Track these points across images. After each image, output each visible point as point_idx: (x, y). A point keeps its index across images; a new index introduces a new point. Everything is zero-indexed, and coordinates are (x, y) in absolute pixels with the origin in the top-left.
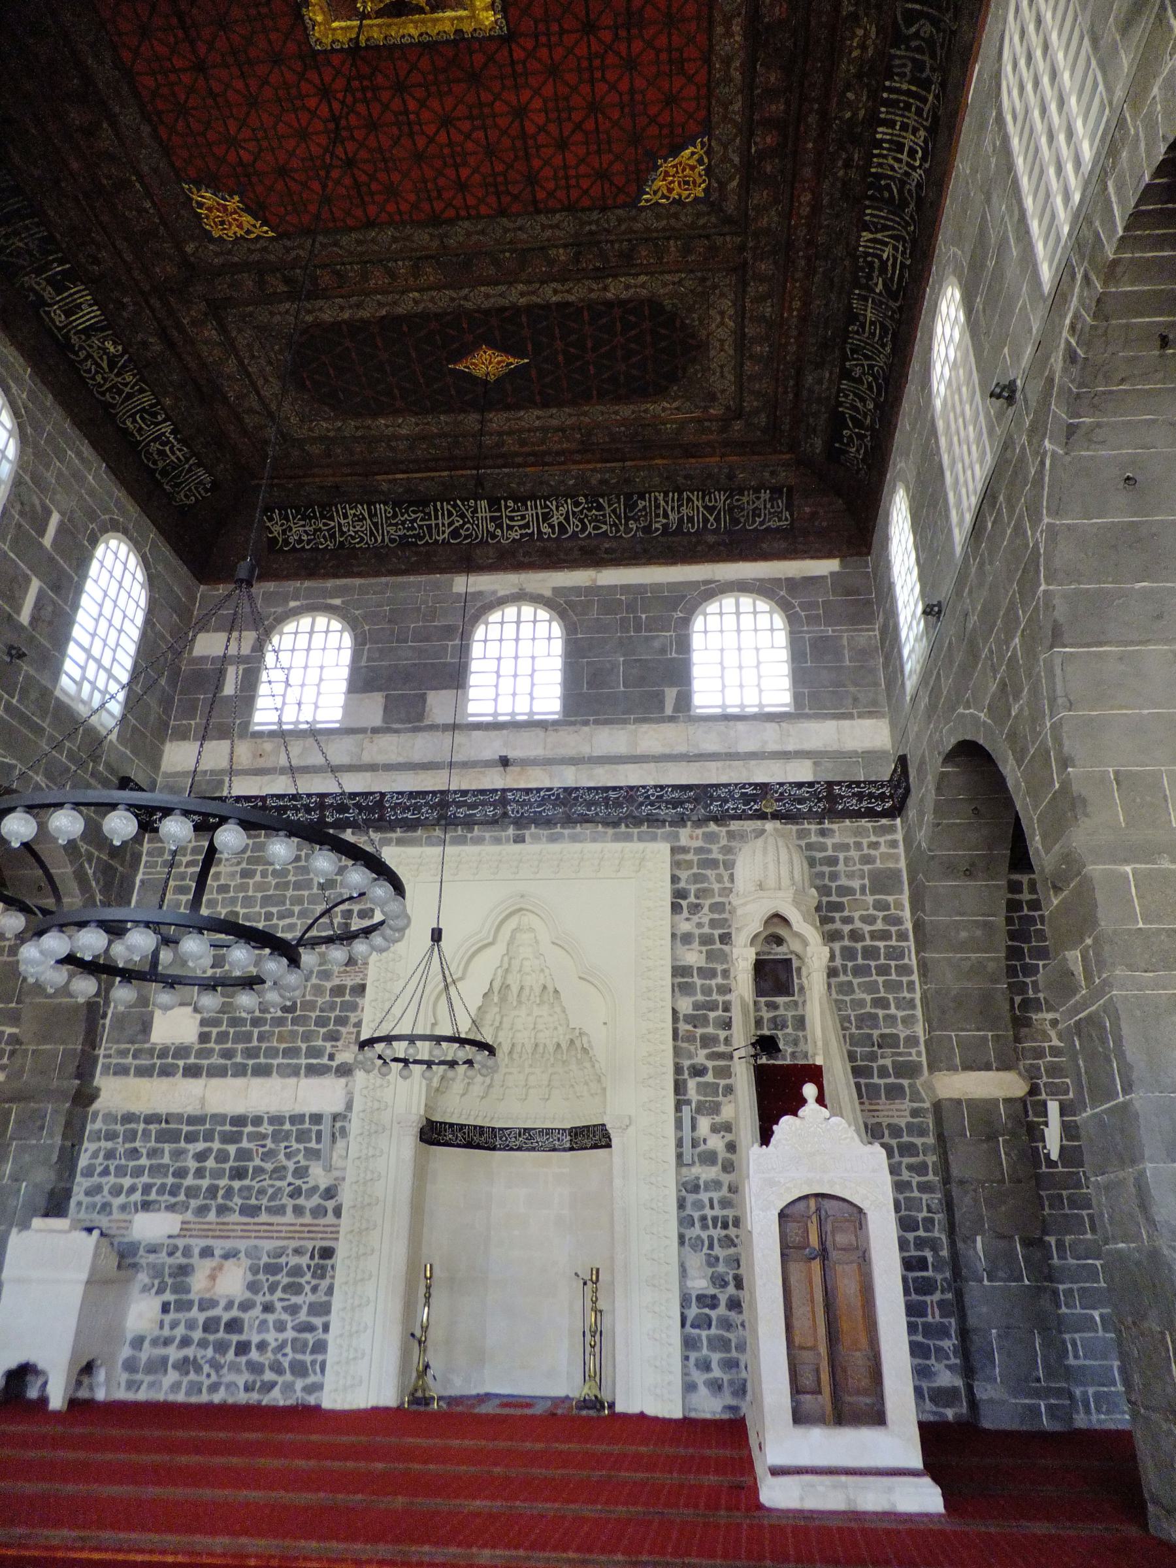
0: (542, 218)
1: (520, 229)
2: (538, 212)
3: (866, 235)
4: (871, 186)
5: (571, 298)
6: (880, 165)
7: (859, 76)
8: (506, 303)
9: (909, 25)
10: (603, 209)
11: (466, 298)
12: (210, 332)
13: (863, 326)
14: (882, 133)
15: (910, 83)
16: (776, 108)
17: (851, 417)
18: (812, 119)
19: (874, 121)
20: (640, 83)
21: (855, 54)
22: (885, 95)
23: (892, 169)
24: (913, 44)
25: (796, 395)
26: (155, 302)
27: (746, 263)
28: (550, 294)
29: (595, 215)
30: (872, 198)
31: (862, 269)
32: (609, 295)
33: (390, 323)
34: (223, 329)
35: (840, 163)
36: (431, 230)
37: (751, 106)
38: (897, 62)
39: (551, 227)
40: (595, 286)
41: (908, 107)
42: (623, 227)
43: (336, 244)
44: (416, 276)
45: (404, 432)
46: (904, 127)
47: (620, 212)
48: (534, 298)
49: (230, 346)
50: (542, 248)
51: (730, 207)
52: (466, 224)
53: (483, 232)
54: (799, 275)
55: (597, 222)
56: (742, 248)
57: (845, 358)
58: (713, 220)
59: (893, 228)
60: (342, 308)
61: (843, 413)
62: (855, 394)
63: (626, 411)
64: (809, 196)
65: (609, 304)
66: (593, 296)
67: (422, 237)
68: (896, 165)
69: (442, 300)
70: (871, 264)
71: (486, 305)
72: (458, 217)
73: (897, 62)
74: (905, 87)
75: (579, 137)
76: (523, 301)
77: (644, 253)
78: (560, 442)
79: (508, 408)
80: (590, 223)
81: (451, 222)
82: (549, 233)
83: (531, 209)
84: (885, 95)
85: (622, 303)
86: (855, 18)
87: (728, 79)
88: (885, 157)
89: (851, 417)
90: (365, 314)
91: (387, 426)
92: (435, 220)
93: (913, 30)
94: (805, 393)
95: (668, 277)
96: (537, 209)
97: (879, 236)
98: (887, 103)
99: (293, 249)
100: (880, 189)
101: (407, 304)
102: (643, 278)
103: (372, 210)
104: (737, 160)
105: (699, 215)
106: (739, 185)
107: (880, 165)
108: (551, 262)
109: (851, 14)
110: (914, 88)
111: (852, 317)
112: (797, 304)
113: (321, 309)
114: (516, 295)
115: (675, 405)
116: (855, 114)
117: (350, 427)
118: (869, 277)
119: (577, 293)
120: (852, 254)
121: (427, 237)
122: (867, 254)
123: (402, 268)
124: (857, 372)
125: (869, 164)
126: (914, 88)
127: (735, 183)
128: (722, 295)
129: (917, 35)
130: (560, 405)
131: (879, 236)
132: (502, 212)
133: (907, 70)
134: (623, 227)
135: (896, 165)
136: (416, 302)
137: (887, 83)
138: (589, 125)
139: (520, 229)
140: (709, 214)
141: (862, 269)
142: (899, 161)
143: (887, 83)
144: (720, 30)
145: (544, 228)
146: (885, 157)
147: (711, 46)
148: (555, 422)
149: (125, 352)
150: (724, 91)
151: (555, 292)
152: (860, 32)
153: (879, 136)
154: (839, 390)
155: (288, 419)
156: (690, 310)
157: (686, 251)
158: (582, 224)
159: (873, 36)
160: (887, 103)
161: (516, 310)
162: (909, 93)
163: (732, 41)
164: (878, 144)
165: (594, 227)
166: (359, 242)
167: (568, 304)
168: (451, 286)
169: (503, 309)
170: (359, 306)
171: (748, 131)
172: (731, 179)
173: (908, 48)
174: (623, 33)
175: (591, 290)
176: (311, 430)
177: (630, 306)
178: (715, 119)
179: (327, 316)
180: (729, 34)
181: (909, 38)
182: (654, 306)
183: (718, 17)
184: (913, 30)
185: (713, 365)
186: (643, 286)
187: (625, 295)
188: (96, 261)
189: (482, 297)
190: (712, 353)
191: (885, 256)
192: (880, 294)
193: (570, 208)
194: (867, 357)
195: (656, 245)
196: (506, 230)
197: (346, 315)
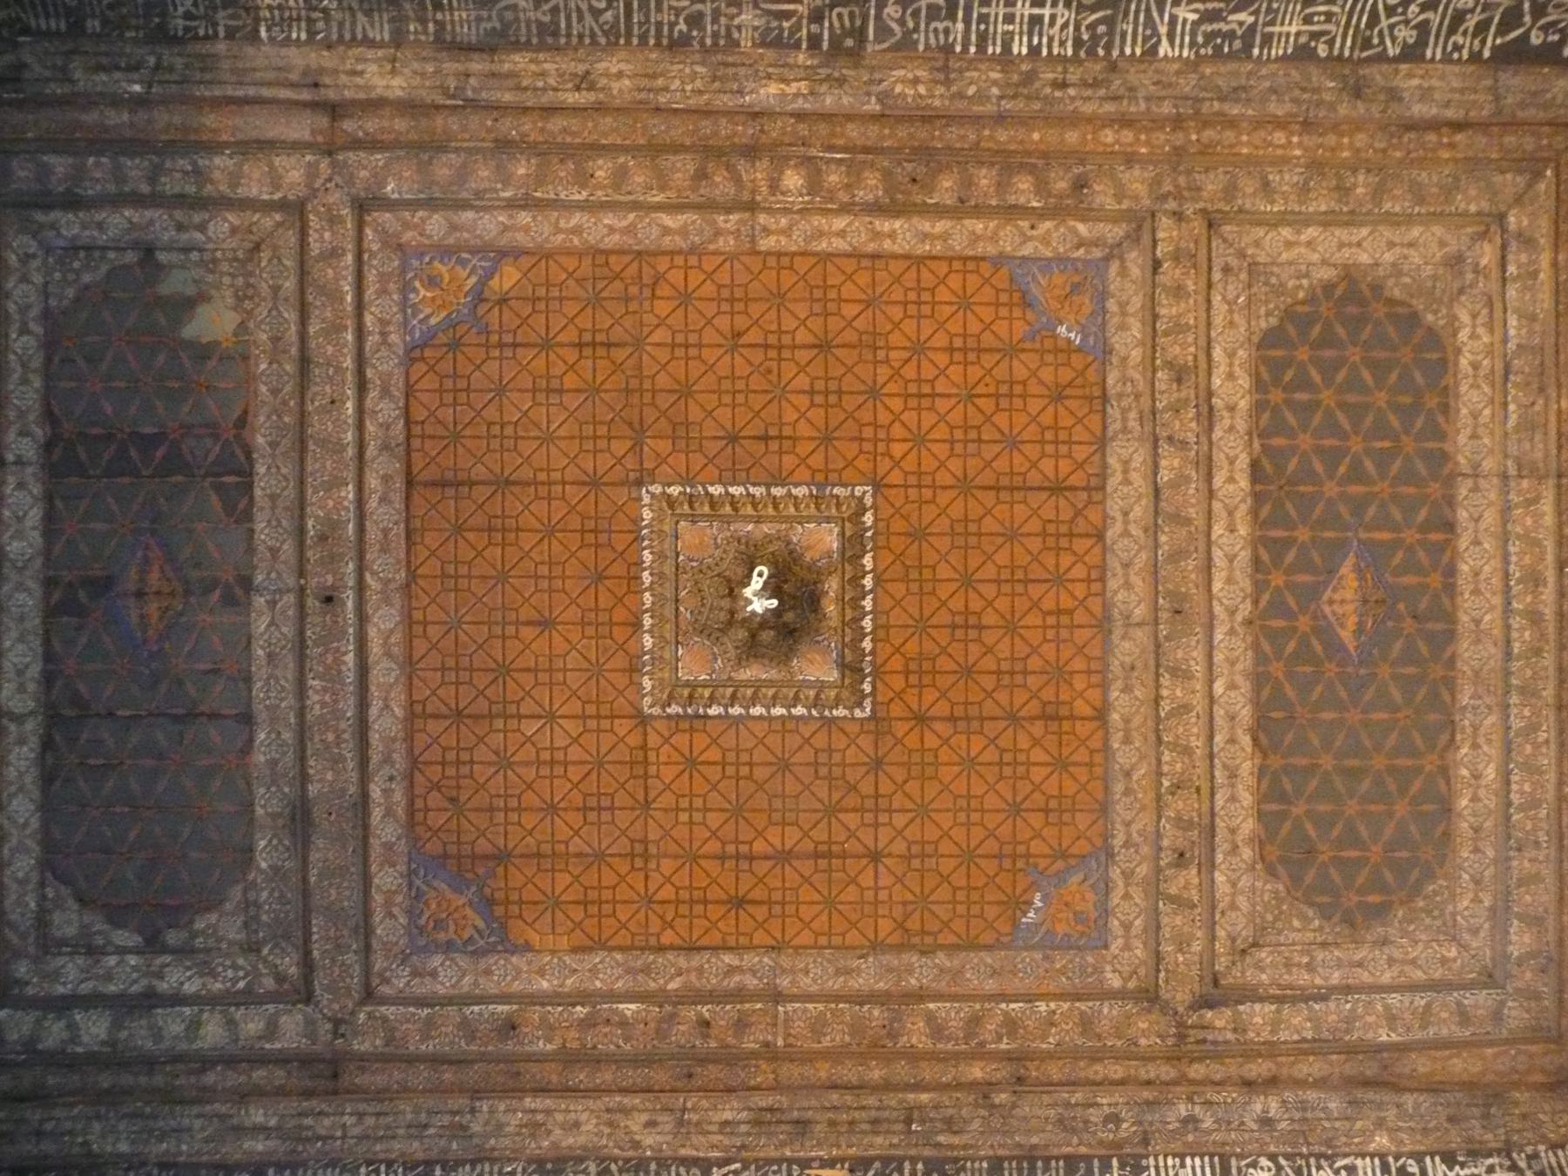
0: (1113, 482)
1: (1126, 514)
2: (1102, 488)
3: (1164, 49)
4: (1092, 53)
5: (1243, 461)
6: (1062, 44)
7: (947, 82)
8: (1244, 556)
9: (891, 32)
10: (1104, 398)
11: (1232, 612)
12: (1258, 1014)
13: (1315, 36)
14: (1020, 48)
15: (954, 21)
16: (985, 179)
17: (1501, 31)
18: (1002, 135)
19: (1006, 59)
20: (940, 340)
21: (922, 89)
22: (973, 49)
23: (1065, 26)
24: (911, 25)
25: (1458, 126)
26: (1197, 1071)
27: (1204, 211)
28: (1234, 485)
29: (1114, 412)
30: (1108, 47)
31: (1218, 49)
32: (1243, 404)
33: (1265, 732)
34: (1251, 994)
35: (1058, 94)
36: (1116, 637)
37: (979, 211)
38: (932, 41)
39: (1125, 472)
40: (1227, 422)
41: (983, 18)
42: (1137, 376)
43: (1128, 774)
44: (1188, 676)
45: (1490, 773)
46: (1009, 19)
47: (1110, 381)
48: (1238, 515)
49: (1288, 997)
50: (1157, 491)
51: (1114, 232)
52: (1112, 584)
53: (1126, 566)
54: (1229, 135)
55: (1124, 411)
56: (1178, 216)
57: (1382, 58)
58: (1134, 254)
59: (1148, 10)
60: (1233, 799)
61: (1494, 47)
62: (1452, 30)
63: (1472, 398)
64: (1108, 131)
65: (1259, 407)
66: (1241, 425)
67: (1127, 648)
68: (1060, 22)
69: (1232, 646)
70: (1209, 37)
71: (1246, 584)
72: (1103, 593)
73: (932, 41)
74: (960, 26)
75: (1002, 420)
76: (1243, 531)
77: (1177, 349)
78: (1537, 517)
79: (1451, 589)
80: (1125, 420)
81: (1106, 607)
82: (1134, 476)
83: (1097, 497)
84: (973, 49)
85: (1259, 385)
86: (882, 98)
87: (945, 236)
88: (1051, 39)
89: (1501, 31)
90: (1246, 768)
91: (1475, 799)
92: (1103, 625)
93: (894, 26)
94: (1450, 114)
95: (1218, 320)
96: (1097, 487)
97: (1163, 30)
98: (981, 48)
99: (1129, 835)
100: (1095, 38)
101: (1235, 700)
102: (1218, 353)
103: (1081, 708)
104: (1048, 224)
105: (1123, 272)
106: (1083, 220)
107: (1062, 44)
108: (1180, 481)
109: (879, 100)
110: (960, 14)
111: (1303, 54)
112: (1279, 137)
113: (1233, 831)
114: (1232, 541)
115: (1465, 317)
116: (995, 83)
117: (1472, 859)
118: (1231, 35)
119: (1233, 450)
120: (1193, 65)
121: (1127, 645)
122: (1193, 44)
123: (1172, 691)
124: (1407, 35)
125: (1062, 59)
126: (960, 14)
127: (1082, 228)
128: (1257, 244)
129: (901, 22)
130: (1451, 501)
131: (1163, 30)
132: (1100, 536)
133: (941, 26)
134: (1137, 376)
135: (1060, 22)
136: (1232, 686)
137: (958, 49)
138: (987, 405)
139: (1126, 514)
140: (1122, 260)
141: (1218, 49)
142: (1053, 18)
143: (958, 49)
144: (887, 245)
145: (1127, 482)
146: (1051, 39)
147: (906, 257)
148: (1490, 518)
149: (1273, 1157)
150: (958, 244)
151: (1231, 480)
152: (898, 89)
153: (1025, 51)
154: (1447, 59)
155: (1444, 961)
156: (1280, 290)
157: (1178, 292)
158: (1125, 430)
159: (902, 72)
160: (981, 48)
161: (1256, 542)
162: (967, 21)
163: (901, 234)
164: (1034, 51)
165: (1133, 415)
166: (1127, 740)
167: (1255, 466)
168: (1210, 628)
169: (1256, 562)
170: (1233, 775)
171: (1012, 212)
172: (1074, 231)
173: (916, 29)
174: (881, 354)
175: (1232, 428)
176: (1475, 932)
177: (1265, 376)
178: (991, 250)
179: (1248, 826)
180: (892, 235)
181: (907, 34)
182: (1270, 339)
183: (871, 247)
184: (894, 26)
185: (1388, 257)
186: (1231, 355)
187: (1244, 381)
188: (1115, 1119)
189: (1231, 588)
190: (1364, 258)
191: (1193, 17)
192: (1256, 13)
193: (1102, 443)
194: (1374, 19)
195: (1166, 334)
196: (1126, 533)
197: (1247, 799)
